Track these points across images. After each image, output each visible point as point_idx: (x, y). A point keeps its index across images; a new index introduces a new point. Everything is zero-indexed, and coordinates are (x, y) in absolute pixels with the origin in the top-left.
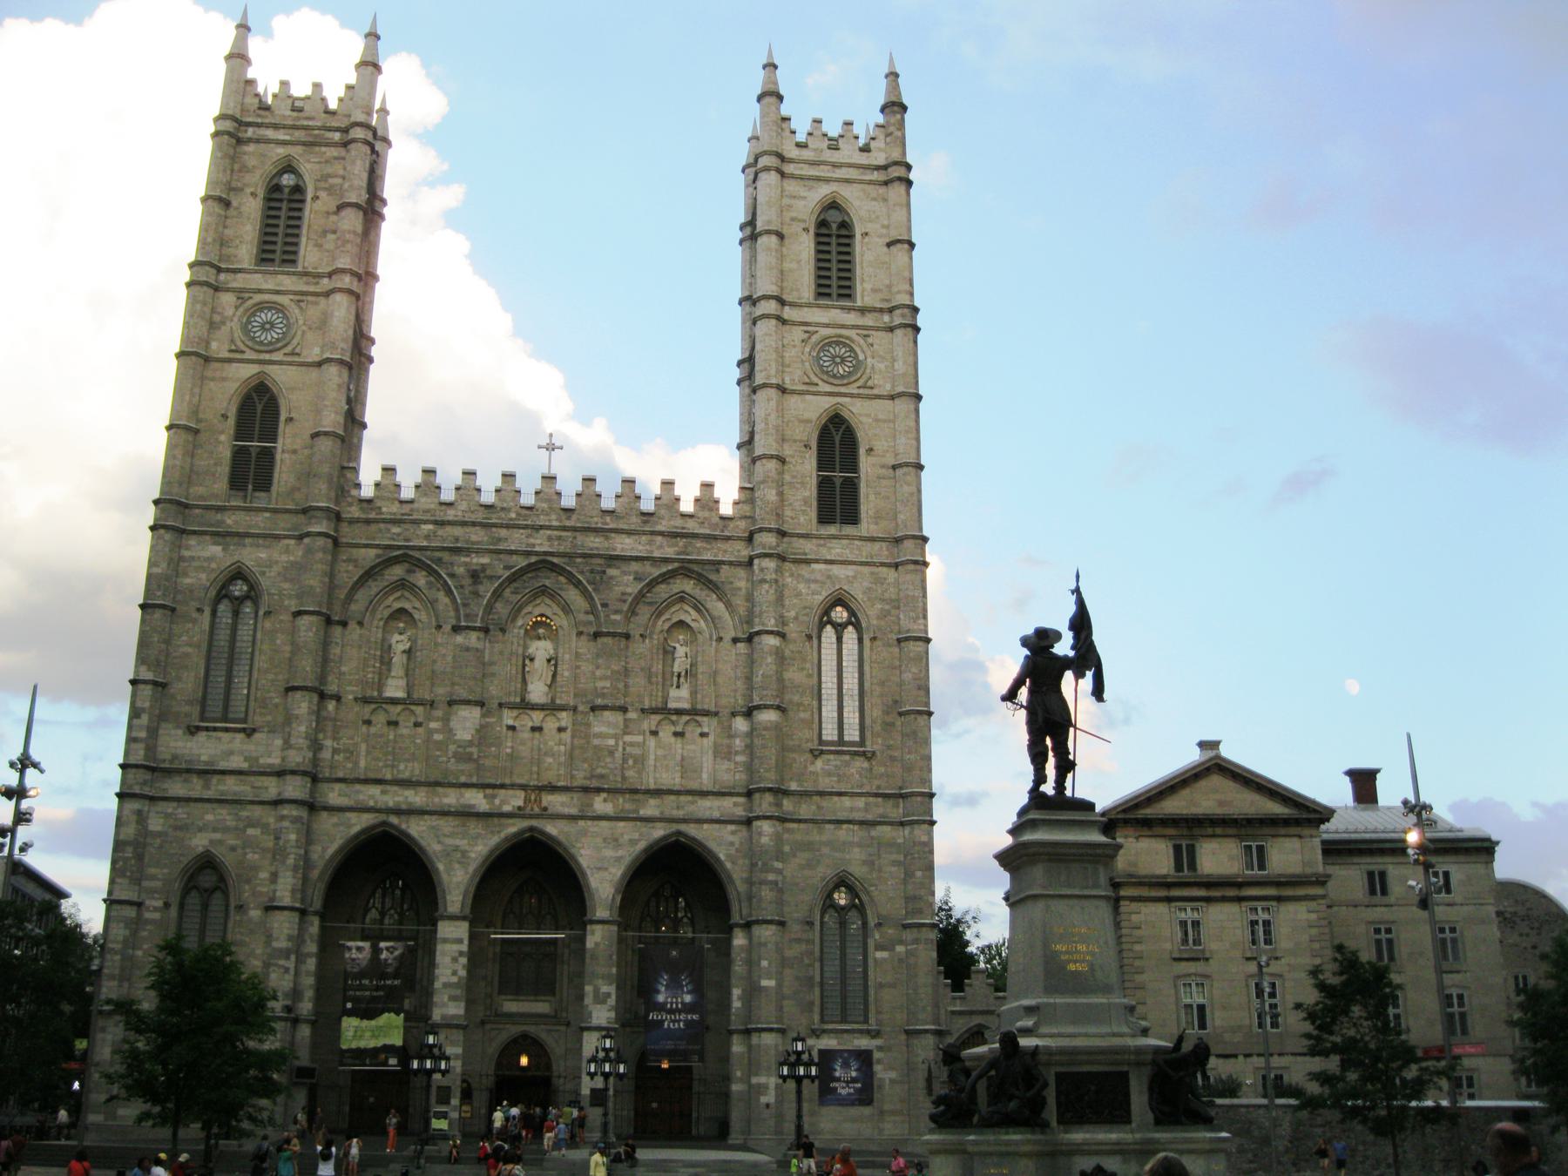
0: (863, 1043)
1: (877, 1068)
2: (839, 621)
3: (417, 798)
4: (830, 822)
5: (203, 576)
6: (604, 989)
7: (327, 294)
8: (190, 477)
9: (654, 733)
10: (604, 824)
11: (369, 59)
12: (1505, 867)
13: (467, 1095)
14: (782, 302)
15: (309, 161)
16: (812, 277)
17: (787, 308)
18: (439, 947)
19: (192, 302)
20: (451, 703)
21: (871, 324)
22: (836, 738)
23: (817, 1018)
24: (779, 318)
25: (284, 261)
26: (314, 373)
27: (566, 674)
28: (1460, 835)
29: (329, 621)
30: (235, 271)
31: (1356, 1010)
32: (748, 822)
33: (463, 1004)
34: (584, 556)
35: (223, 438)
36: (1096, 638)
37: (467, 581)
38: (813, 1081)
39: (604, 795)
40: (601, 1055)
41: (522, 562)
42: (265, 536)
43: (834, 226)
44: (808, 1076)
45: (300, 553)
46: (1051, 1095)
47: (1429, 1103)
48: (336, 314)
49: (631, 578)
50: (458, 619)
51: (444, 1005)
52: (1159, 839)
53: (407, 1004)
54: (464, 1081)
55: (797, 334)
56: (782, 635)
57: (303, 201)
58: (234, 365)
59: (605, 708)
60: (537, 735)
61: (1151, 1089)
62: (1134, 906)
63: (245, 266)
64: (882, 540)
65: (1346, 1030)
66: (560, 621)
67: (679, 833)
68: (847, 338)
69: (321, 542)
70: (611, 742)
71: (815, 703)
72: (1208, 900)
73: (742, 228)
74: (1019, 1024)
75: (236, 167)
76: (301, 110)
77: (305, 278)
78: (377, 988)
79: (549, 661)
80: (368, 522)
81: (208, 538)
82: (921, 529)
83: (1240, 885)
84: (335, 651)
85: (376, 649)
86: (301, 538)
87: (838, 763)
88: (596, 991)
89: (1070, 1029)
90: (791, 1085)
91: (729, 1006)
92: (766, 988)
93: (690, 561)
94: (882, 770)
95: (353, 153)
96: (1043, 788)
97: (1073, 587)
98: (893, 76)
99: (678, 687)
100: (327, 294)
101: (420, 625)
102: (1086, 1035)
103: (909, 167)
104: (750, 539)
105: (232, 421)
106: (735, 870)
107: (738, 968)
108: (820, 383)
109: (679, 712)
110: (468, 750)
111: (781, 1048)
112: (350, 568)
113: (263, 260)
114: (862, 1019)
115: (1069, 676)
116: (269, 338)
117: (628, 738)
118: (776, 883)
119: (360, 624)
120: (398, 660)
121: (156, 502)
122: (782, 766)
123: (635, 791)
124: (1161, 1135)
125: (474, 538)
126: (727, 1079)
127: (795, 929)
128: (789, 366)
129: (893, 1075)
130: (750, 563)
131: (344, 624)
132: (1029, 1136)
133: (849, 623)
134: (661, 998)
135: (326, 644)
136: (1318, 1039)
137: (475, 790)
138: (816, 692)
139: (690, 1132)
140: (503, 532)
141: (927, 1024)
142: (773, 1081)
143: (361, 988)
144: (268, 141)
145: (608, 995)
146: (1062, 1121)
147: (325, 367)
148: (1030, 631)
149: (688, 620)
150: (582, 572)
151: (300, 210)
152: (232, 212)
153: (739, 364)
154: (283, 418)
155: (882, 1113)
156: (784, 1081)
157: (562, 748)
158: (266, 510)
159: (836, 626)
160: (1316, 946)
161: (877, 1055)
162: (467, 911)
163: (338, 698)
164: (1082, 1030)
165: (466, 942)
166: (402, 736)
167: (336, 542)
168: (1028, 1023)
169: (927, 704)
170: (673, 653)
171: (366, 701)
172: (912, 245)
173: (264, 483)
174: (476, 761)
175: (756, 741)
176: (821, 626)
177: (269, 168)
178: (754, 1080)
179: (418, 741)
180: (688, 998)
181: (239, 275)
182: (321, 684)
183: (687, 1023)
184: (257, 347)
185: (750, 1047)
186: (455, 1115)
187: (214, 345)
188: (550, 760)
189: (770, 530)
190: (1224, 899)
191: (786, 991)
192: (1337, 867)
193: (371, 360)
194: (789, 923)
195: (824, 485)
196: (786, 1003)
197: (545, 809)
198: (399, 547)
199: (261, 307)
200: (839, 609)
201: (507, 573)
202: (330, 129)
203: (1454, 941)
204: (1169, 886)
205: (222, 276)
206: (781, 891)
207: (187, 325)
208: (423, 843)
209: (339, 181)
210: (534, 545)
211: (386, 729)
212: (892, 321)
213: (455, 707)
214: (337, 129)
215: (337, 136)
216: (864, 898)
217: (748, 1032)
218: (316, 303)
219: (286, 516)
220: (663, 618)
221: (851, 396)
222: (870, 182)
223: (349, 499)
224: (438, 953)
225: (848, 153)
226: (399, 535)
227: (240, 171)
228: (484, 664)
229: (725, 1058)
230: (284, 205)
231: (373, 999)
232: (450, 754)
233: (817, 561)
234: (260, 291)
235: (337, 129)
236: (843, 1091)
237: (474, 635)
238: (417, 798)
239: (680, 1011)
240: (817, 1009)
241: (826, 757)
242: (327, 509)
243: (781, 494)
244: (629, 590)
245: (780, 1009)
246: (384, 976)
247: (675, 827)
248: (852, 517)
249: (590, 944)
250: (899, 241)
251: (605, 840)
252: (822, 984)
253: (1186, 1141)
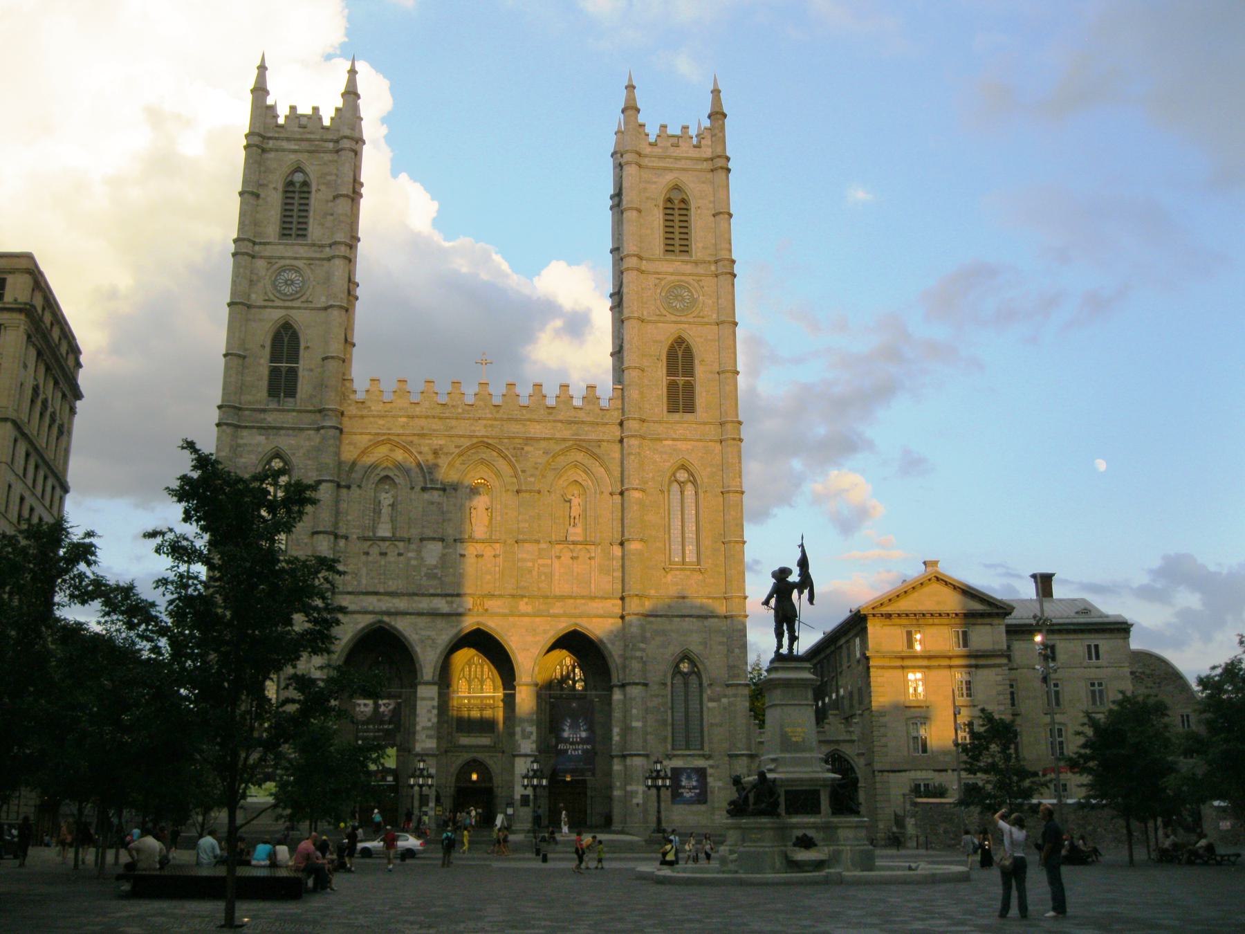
0: (700, 763)
1: (710, 779)
2: (682, 479)
3: (401, 604)
4: (678, 616)
5: (253, 457)
6: (529, 729)
7: (329, 259)
8: (241, 388)
9: (559, 557)
10: (526, 619)
11: (351, 89)
12: (1135, 644)
13: (438, 800)
14: (640, 258)
15: (312, 164)
16: (662, 239)
17: (644, 262)
18: (419, 703)
19: (236, 266)
20: (422, 540)
21: (702, 272)
22: (681, 559)
23: (669, 747)
24: (638, 270)
25: (298, 235)
26: (323, 314)
27: (499, 518)
28: (1106, 620)
29: (339, 486)
30: (265, 244)
31: (994, 747)
32: (622, 617)
33: (435, 741)
34: (509, 438)
35: (262, 361)
36: (810, 571)
37: (430, 457)
38: (667, 789)
39: (525, 600)
40: (531, 774)
41: (467, 443)
42: (293, 429)
43: (676, 202)
44: (664, 786)
45: (318, 440)
46: (782, 800)
47: (1035, 801)
48: (337, 273)
49: (541, 452)
50: (426, 483)
51: (423, 741)
52: (896, 627)
53: (399, 738)
54: (437, 791)
55: (652, 280)
56: (643, 490)
57: (309, 192)
58: (269, 310)
59: (524, 541)
60: (480, 559)
61: (830, 797)
62: (880, 672)
63: (271, 240)
64: (711, 423)
65: (985, 760)
66: (494, 482)
67: (577, 624)
68: (687, 282)
69: (332, 432)
70: (530, 564)
71: (667, 536)
72: (928, 667)
73: (612, 197)
74: (768, 767)
75: (263, 169)
76: (305, 127)
77: (313, 248)
78: (379, 730)
79: (487, 509)
80: (362, 417)
81: (255, 430)
82: (737, 415)
83: (950, 658)
84: (343, 506)
85: (370, 504)
86: (318, 429)
88: (523, 731)
89: (792, 769)
90: (654, 791)
91: (611, 739)
92: (636, 728)
93: (580, 440)
94: (712, 580)
95: (343, 158)
96: (781, 651)
97: (800, 544)
98: (716, 92)
99: (574, 526)
100: (329, 259)
101: (399, 486)
102: (800, 772)
103: (728, 159)
104: (621, 424)
105: (268, 350)
106: (615, 652)
107: (617, 714)
108: (667, 314)
109: (574, 543)
110: (435, 571)
111: (646, 767)
112: (351, 449)
113: (284, 235)
114: (699, 747)
115: (795, 593)
116: (291, 291)
117: (540, 561)
118: (642, 658)
119: (359, 487)
120: (386, 511)
121: (220, 407)
123: (547, 597)
124: (835, 820)
125: (434, 427)
126: (610, 787)
127: (654, 688)
128: (646, 303)
129: (720, 784)
130: (621, 441)
131: (348, 487)
132: (772, 820)
133: (690, 481)
134: (566, 735)
135: (337, 501)
136: (971, 764)
137: (440, 598)
138: (667, 529)
139: (586, 823)
140: (454, 423)
141: (743, 750)
142: (641, 789)
143: (367, 731)
144: (284, 150)
145: (532, 733)
146: (788, 813)
147: (330, 310)
148: (776, 568)
149: (580, 480)
150: (508, 449)
151: (308, 198)
152: (261, 201)
153: (611, 296)
154: (302, 347)
155: (713, 808)
156: (649, 789)
157: (497, 568)
158: (294, 410)
159: (680, 483)
160: (1001, 697)
161: (710, 771)
162: (436, 678)
163: (346, 538)
164: (796, 769)
165: (436, 699)
166: (390, 563)
167: (341, 431)
168: (772, 766)
169: (742, 536)
170: (570, 501)
171: (366, 539)
172: (730, 215)
173: (292, 393)
174: (440, 579)
175: (627, 563)
176: (670, 483)
177: (286, 170)
178: (629, 788)
179: (401, 566)
180: (584, 735)
181: (267, 246)
182: (335, 529)
183: (583, 750)
184: (283, 298)
185: (625, 766)
186: (432, 813)
187: (253, 296)
188: (489, 577)
189: (635, 419)
190: (939, 667)
191: (649, 729)
192: (1021, 642)
193: (357, 298)
194: (650, 685)
195: (672, 387)
196: (649, 737)
197: (487, 610)
198: (384, 434)
199: (284, 269)
200: (682, 471)
201: (457, 451)
202: (326, 141)
203: (1101, 692)
204: (903, 658)
205: (257, 248)
206: (645, 663)
207: (234, 283)
208: (406, 634)
209: (334, 178)
210: (474, 431)
211: (379, 558)
212: (717, 270)
213: (425, 542)
214: (331, 141)
215: (331, 145)
216: (700, 667)
217: (624, 757)
218: (323, 265)
219: (309, 415)
220: (563, 479)
221: (690, 323)
222: (701, 170)
223: (349, 402)
224: (418, 707)
225: (685, 150)
226: (384, 425)
227: (265, 172)
228: (443, 513)
229: (609, 773)
230: (297, 196)
231: (375, 738)
232: (423, 574)
233: (666, 440)
234: (283, 258)
235: (331, 141)
236: (687, 794)
237: (436, 493)
238: (401, 604)
239: (578, 743)
240: (670, 740)
241: (673, 572)
242: (335, 410)
243: (641, 393)
244: (539, 461)
245: (645, 741)
246: (382, 723)
247: (573, 620)
248: (690, 408)
249: (518, 699)
250: (721, 213)
251: (527, 630)
252: (673, 725)
253: (846, 822)
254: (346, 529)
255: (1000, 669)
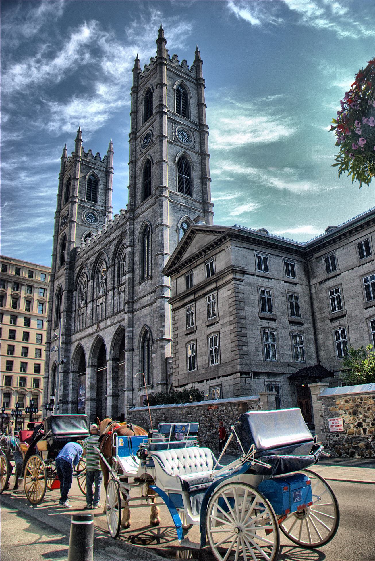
3: (82, 334)
10: (109, 328)
33: (90, 393)
39: (109, 319)
87: (145, 285)
122: (132, 292)
125: (91, 253)
127: (136, 351)
131: (76, 290)
145: (110, 385)
160: (231, 309)
190: (200, 297)
237: (91, 281)
238: (82, 334)
254: (75, 308)
255: (230, 285)
